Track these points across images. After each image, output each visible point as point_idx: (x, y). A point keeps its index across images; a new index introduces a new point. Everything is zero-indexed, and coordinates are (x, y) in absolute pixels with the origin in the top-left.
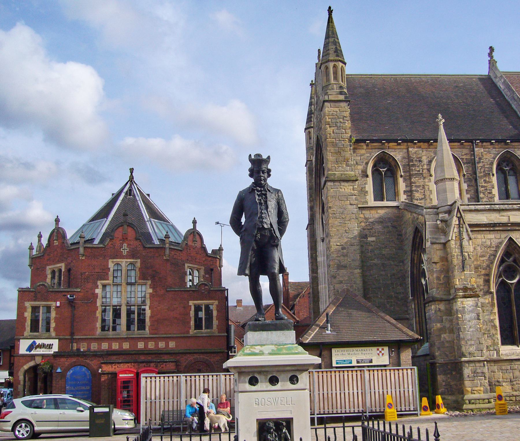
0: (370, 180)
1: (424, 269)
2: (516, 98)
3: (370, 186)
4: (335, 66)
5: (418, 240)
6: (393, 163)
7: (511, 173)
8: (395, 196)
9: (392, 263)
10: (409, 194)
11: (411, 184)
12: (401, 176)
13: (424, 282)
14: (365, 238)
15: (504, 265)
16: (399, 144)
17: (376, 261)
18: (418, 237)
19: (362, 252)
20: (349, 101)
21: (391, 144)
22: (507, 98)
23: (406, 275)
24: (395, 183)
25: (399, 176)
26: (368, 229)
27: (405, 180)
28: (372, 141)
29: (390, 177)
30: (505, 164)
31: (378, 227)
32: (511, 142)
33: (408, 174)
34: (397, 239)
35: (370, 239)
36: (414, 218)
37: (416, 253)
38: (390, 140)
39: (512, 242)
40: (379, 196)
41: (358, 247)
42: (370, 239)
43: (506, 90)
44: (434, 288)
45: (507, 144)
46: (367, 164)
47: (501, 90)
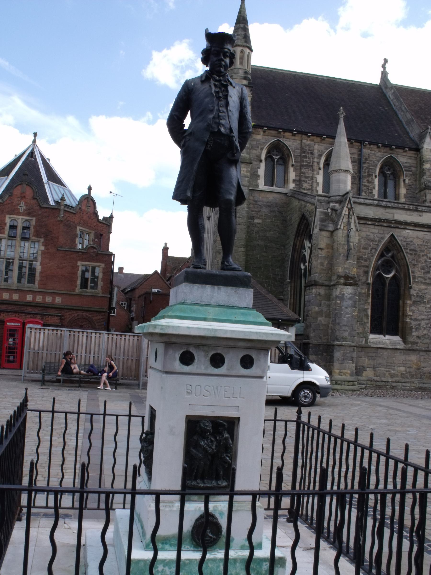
0: (263, 165)
1: (304, 255)
2: (403, 108)
3: (262, 172)
5: (302, 227)
6: (286, 152)
7: (392, 177)
8: (285, 182)
9: (274, 246)
10: (298, 183)
11: (300, 174)
12: (293, 165)
13: (303, 267)
14: (251, 219)
15: (382, 259)
16: (294, 135)
17: (259, 242)
18: (304, 224)
19: (248, 232)
20: (252, 87)
21: (287, 134)
22: (394, 108)
23: (286, 259)
24: (286, 172)
25: (290, 165)
26: (256, 212)
27: (295, 170)
28: (270, 128)
29: (282, 165)
30: (387, 168)
31: (265, 210)
32: (396, 148)
33: (299, 164)
34: (282, 224)
35: (256, 221)
36: (302, 205)
37: (299, 238)
38: (287, 130)
39: (393, 239)
40: (270, 181)
41: (245, 227)
42: (256, 221)
43: (395, 100)
44: (317, 273)
45: (392, 149)
46: (262, 149)
47: (390, 100)
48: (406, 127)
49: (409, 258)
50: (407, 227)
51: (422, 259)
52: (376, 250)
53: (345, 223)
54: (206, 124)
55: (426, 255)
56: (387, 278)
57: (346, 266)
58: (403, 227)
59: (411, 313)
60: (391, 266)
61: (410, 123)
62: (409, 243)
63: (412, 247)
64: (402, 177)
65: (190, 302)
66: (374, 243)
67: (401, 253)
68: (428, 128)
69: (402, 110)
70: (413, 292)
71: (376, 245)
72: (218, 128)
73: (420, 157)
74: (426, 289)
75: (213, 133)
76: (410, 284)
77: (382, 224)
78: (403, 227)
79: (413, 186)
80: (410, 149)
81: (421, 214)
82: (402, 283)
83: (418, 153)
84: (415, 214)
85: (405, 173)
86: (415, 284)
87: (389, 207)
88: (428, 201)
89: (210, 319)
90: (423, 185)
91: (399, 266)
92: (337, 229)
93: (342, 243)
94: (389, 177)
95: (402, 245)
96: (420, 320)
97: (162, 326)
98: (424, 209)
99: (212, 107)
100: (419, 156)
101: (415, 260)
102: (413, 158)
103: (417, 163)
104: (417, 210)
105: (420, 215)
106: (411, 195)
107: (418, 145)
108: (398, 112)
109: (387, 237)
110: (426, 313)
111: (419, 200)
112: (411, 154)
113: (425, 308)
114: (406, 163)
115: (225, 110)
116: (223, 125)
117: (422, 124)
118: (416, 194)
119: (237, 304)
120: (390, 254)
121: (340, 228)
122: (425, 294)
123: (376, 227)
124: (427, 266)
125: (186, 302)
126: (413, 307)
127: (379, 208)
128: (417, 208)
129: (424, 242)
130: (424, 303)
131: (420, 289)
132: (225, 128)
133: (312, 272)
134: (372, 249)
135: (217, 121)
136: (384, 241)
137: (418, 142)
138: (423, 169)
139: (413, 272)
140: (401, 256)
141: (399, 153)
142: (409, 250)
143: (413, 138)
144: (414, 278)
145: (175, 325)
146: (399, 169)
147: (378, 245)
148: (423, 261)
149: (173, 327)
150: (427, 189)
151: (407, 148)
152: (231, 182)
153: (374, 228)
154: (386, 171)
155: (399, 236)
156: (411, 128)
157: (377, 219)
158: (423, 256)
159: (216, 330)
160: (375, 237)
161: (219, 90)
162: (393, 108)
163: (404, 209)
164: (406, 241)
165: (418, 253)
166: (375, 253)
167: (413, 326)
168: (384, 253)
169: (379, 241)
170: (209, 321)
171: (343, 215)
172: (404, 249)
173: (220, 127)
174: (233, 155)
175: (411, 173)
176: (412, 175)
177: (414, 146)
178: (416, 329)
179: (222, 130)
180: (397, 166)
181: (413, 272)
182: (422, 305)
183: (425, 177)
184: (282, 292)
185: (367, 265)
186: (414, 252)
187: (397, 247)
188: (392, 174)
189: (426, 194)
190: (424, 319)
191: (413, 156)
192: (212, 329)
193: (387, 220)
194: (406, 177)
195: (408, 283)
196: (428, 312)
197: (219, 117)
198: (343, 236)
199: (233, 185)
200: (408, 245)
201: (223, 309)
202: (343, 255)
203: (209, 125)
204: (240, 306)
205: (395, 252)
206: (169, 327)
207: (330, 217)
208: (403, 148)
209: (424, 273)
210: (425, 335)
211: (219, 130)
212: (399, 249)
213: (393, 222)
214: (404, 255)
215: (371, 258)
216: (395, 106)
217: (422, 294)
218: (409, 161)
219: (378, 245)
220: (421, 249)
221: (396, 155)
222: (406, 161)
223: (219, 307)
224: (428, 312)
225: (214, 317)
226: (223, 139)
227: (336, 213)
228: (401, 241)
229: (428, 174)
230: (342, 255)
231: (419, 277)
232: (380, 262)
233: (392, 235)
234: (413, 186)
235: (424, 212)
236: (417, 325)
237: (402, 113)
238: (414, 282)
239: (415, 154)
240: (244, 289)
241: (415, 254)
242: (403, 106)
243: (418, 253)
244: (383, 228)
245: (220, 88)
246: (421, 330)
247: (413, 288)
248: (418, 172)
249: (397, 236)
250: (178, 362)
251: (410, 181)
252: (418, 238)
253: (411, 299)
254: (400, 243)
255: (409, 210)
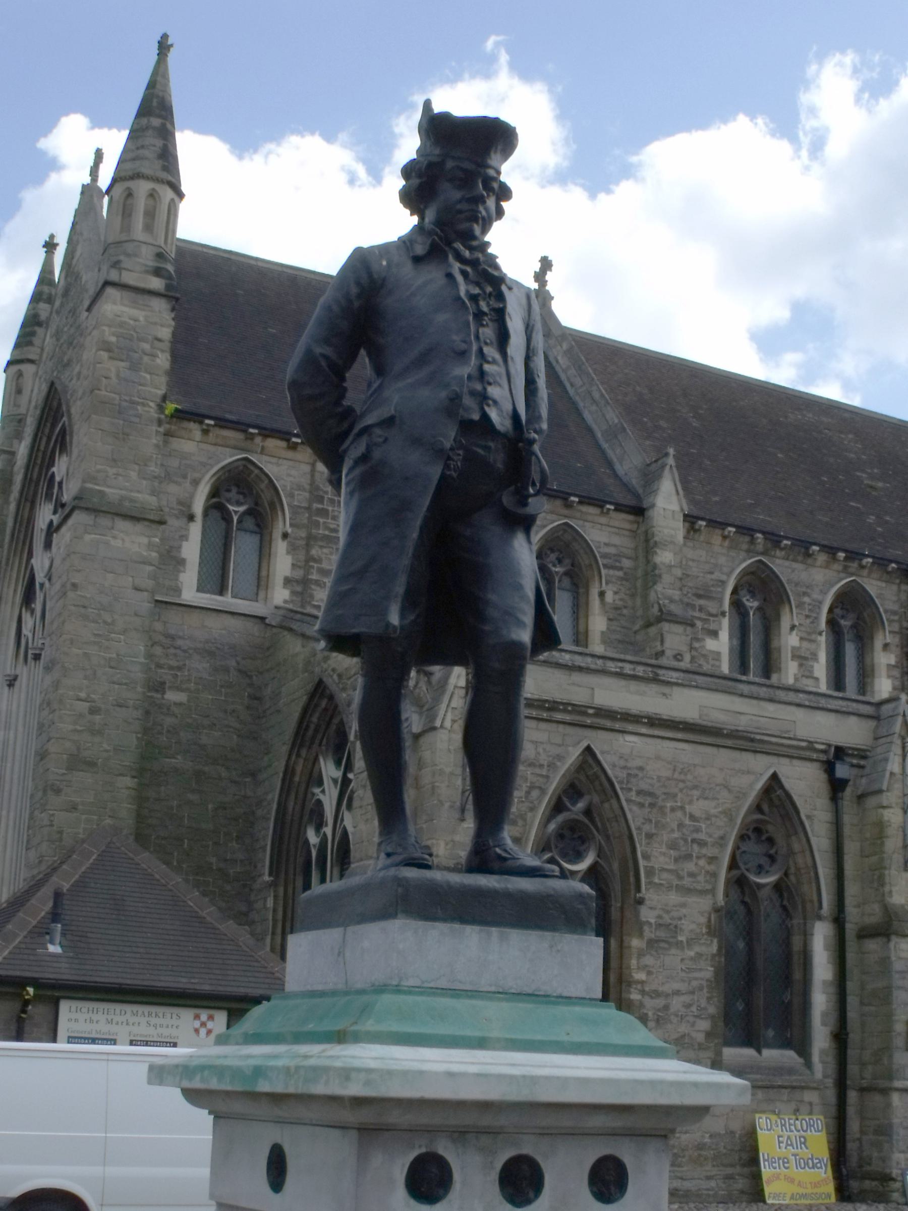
0: (196, 530)
1: (319, 803)
2: (596, 395)
3: (191, 550)
4: (152, 195)
5: (315, 720)
6: (266, 496)
7: (566, 582)
9: (224, 774)
10: (299, 589)
11: (307, 561)
12: (285, 536)
13: (313, 838)
14: (157, 691)
15: (560, 818)
16: (293, 447)
17: (178, 761)
18: (320, 709)
19: (146, 731)
20: (177, 299)
21: (273, 444)
22: (571, 391)
23: (259, 813)
24: (264, 553)
25: (277, 534)
26: (171, 668)
27: (292, 549)
28: (222, 423)
29: (252, 532)
30: (553, 557)
31: (200, 666)
32: (580, 502)
34: (248, 708)
35: (172, 696)
37: (304, 752)
38: (273, 430)
39: (590, 761)
40: (217, 578)
41: (138, 714)
42: (172, 696)
43: (572, 372)
44: (371, 858)
45: (569, 506)
46: (196, 483)
47: (558, 369)
48: (605, 446)
49: (635, 816)
50: (630, 727)
51: (672, 820)
52: (543, 791)
53: (457, 712)
54: (443, 394)
55: (682, 808)
56: (760, 886)
57: (457, 838)
58: (617, 726)
59: (641, 976)
60: (583, 840)
61: (616, 437)
62: (636, 772)
63: (643, 786)
64: (597, 584)
65: (418, 983)
66: (538, 771)
67: (614, 802)
68: (667, 455)
69: (594, 401)
70: (647, 914)
71: (542, 776)
72: (482, 409)
73: (646, 532)
74: (683, 905)
75: (466, 426)
76: (638, 889)
77: (559, 716)
78: (617, 726)
79: (625, 611)
80: (619, 508)
81: (666, 690)
82: (616, 887)
83: (641, 519)
84: (654, 688)
85: (603, 572)
86: (651, 890)
87: (580, 669)
88: (669, 653)
89: (498, 1040)
90: (655, 610)
91: (608, 837)
92: (434, 729)
93: (448, 770)
94: (560, 581)
95: (616, 778)
96: (667, 995)
97: (369, 1071)
98: (673, 676)
99: (465, 342)
100: (642, 529)
101: (650, 821)
102: (627, 533)
103: (636, 549)
104: (656, 680)
105: (664, 694)
106: (618, 637)
107: (638, 497)
108: (581, 405)
109: (574, 754)
110: (683, 974)
111: (644, 650)
112: (622, 520)
113: (682, 960)
114: (606, 544)
115: (498, 356)
116: (495, 402)
117: (648, 443)
118: (635, 632)
119: (557, 987)
120: (581, 805)
121: (442, 726)
122: (680, 919)
123: (543, 725)
124: (686, 841)
125: (404, 983)
126: (648, 957)
127: (550, 670)
128: (657, 675)
129: (674, 770)
130: (679, 945)
131: (666, 905)
132: (500, 410)
133: (354, 854)
134: (532, 787)
135: (478, 387)
136: (567, 766)
137: (640, 491)
138: (655, 564)
139: (646, 857)
140: (611, 808)
141: (590, 518)
142: (633, 793)
143: (625, 479)
144: (650, 872)
145: (407, 1065)
146: (587, 562)
147: (547, 777)
148: (674, 825)
149: (405, 1073)
150: (667, 621)
151: (611, 503)
152: (519, 587)
153: (537, 729)
154: (550, 566)
155: (608, 753)
156: (618, 451)
157: (546, 701)
158: (673, 810)
159: (533, 1080)
160: (539, 753)
161: (476, 291)
162: (567, 392)
163: (620, 675)
164: (625, 768)
165: (660, 803)
166: (540, 802)
167: (650, 1014)
168: (565, 799)
169: (552, 766)
170: (494, 1049)
171: (450, 688)
172: (622, 789)
173: (486, 408)
174: (523, 501)
175: (620, 574)
176: (621, 579)
177: (629, 501)
178: (658, 1021)
179: (493, 414)
180: (581, 551)
181: (646, 857)
182: (673, 951)
183: (659, 587)
184: (246, 914)
185: (518, 835)
186: (649, 800)
187: (601, 784)
188: (566, 574)
189: (662, 635)
190: (677, 993)
191: (627, 526)
192: (524, 1077)
193: (574, 705)
194: (607, 583)
195: (633, 887)
196: (690, 970)
197: (481, 375)
198: (449, 750)
199: (523, 597)
200: (633, 780)
201: (520, 1005)
202: (451, 807)
203: (455, 399)
204: (565, 994)
205: (596, 799)
206: (390, 1073)
207: (412, 692)
208: (599, 503)
209: (676, 860)
210: (683, 1036)
211: (485, 417)
212: (609, 790)
213: (591, 711)
214: (622, 808)
215: (529, 815)
216: (572, 385)
217: (672, 918)
218: (616, 540)
219: (547, 777)
220: (666, 791)
221: (581, 522)
222: (606, 540)
223: (507, 1000)
224: (690, 970)
225: (508, 1036)
226: (492, 444)
227: (429, 682)
228: (614, 766)
229: (667, 579)
230: (447, 805)
231: (663, 870)
232: (552, 827)
233: (588, 749)
234: (625, 611)
235: (677, 684)
236: (659, 1010)
237: (594, 408)
238: (650, 883)
239: (631, 522)
240: (576, 937)
241: (652, 805)
242: (594, 388)
243: (660, 803)
244: (561, 727)
245: (478, 284)
246: (671, 1023)
247: (647, 902)
248: (640, 573)
249: (602, 753)
250: (401, 1192)
251: (617, 597)
252: (658, 758)
253: (641, 935)
254: (609, 772)
255: (634, 677)
